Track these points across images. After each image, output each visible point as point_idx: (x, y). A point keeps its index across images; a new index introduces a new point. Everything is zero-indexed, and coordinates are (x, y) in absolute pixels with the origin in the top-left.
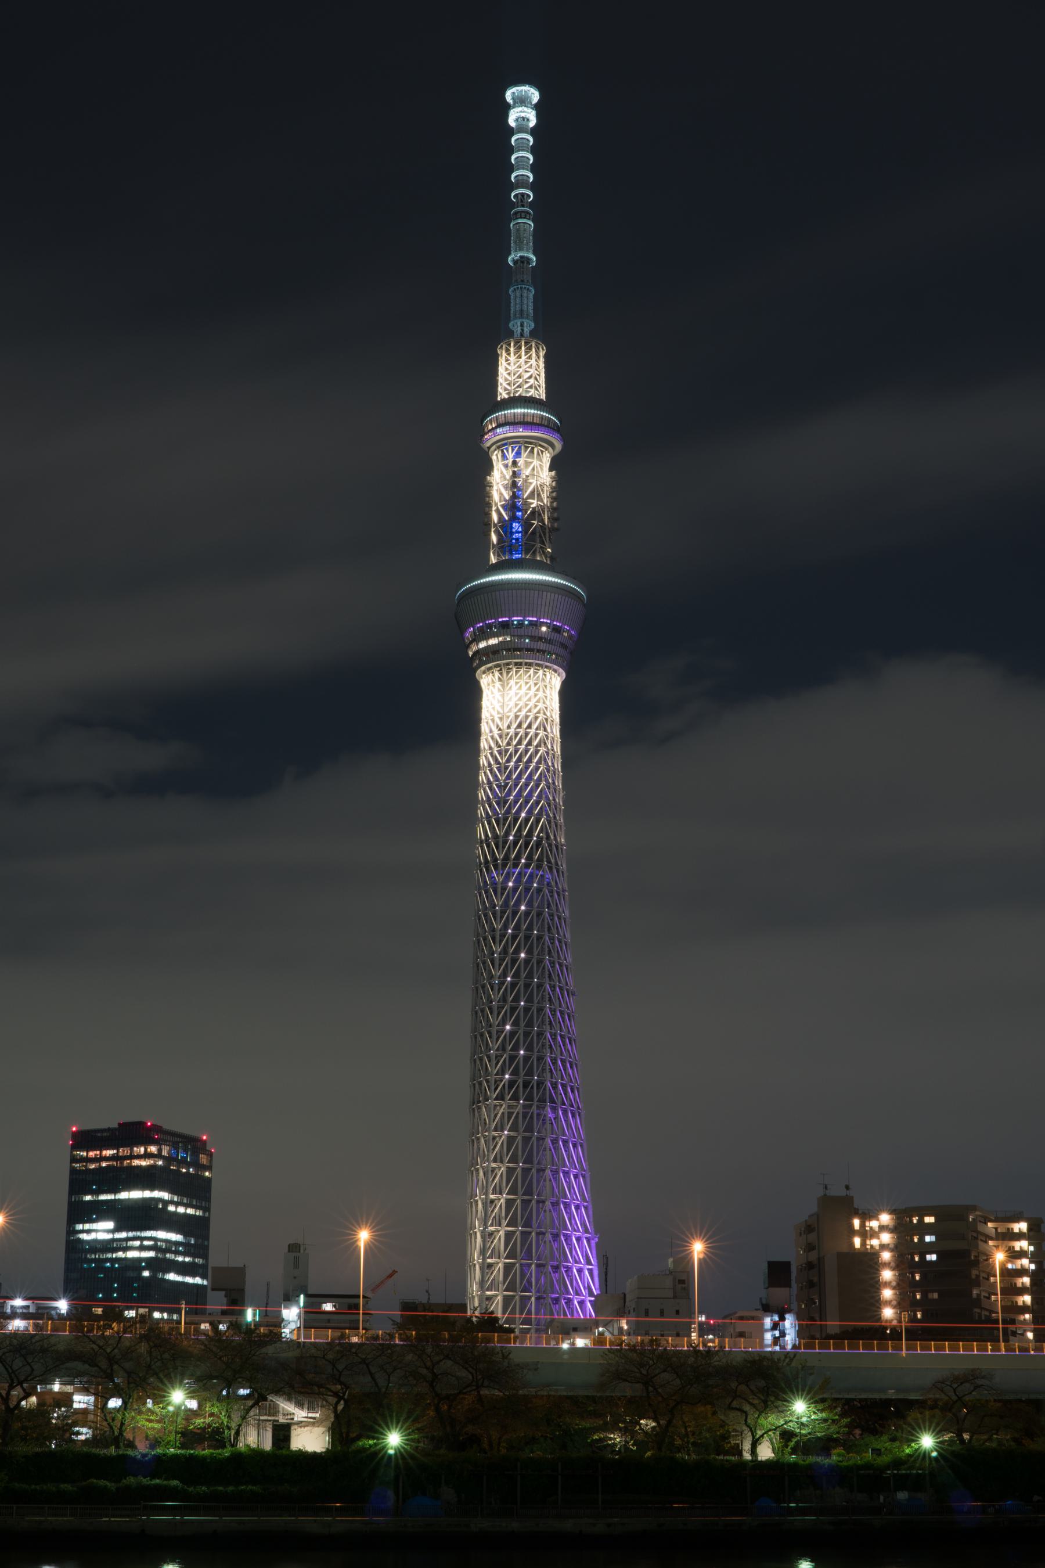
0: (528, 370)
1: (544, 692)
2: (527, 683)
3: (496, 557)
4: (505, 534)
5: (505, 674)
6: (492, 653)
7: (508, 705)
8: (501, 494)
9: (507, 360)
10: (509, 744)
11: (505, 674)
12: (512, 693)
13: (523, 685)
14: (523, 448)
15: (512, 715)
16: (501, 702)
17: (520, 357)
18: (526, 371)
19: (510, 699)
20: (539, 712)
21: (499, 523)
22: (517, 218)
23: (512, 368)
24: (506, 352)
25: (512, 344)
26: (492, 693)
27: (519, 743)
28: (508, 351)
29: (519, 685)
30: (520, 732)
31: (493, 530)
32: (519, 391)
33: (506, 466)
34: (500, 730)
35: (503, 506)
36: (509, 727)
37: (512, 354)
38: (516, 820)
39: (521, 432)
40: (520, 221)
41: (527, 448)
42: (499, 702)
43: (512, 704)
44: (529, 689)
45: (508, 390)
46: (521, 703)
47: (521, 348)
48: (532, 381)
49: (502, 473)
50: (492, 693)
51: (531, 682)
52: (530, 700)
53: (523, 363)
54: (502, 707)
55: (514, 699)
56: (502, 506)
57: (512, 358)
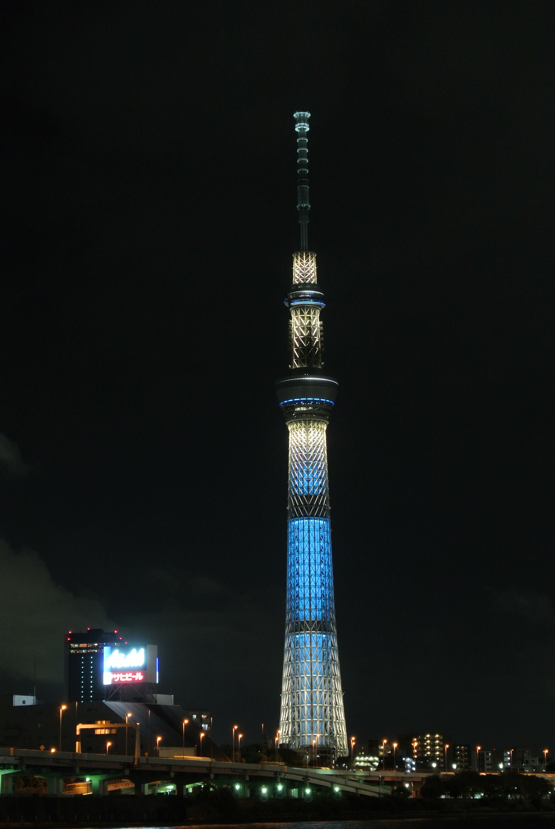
0: (312, 268)
1: (323, 434)
2: (318, 430)
3: (299, 364)
4: (305, 354)
5: (307, 425)
6: (301, 413)
7: (309, 441)
8: (301, 331)
9: (301, 261)
10: (311, 460)
11: (307, 425)
12: (311, 434)
13: (316, 431)
14: (312, 310)
15: (312, 445)
16: (306, 438)
17: (308, 261)
18: (312, 269)
19: (311, 438)
20: (322, 445)
21: (299, 346)
22: (302, 184)
24: (300, 257)
25: (304, 254)
26: (300, 433)
27: (315, 460)
28: (302, 257)
29: (314, 431)
30: (315, 454)
31: (294, 349)
32: (309, 279)
33: (303, 318)
34: (305, 452)
35: (303, 339)
36: (310, 452)
37: (304, 259)
38: (315, 497)
39: (311, 302)
40: (303, 186)
41: (313, 310)
42: (304, 438)
43: (311, 440)
44: (318, 433)
45: (302, 277)
46: (316, 440)
47: (309, 256)
48: (314, 274)
49: (300, 320)
50: (300, 433)
51: (319, 430)
52: (319, 439)
53: (310, 265)
54: (307, 440)
55: (313, 438)
56: (302, 339)
57: (304, 261)
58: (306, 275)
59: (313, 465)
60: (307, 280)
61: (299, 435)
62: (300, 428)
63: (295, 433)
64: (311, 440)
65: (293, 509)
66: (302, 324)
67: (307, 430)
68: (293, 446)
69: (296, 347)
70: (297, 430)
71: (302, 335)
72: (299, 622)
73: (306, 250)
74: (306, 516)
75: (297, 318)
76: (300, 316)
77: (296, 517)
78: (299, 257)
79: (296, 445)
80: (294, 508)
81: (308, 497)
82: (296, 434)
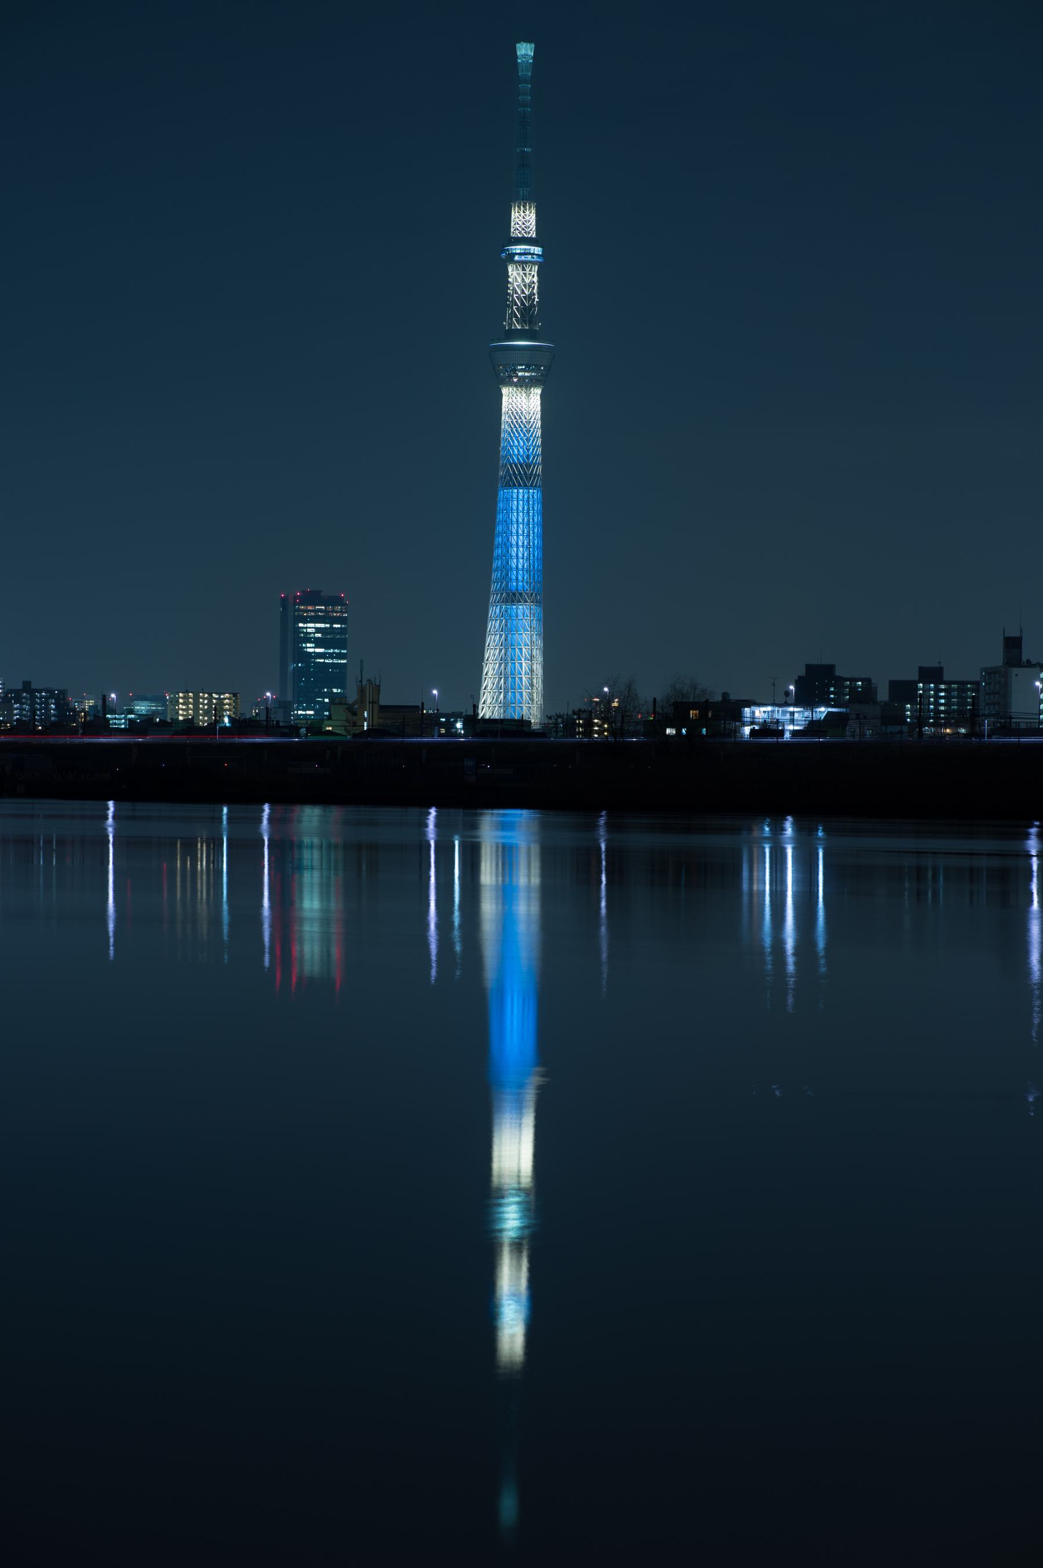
8: (522, 289)
10: (530, 428)
12: (531, 401)
15: (532, 412)
23: (527, 218)
27: (535, 428)
33: (525, 274)
36: (530, 419)
42: (525, 404)
49: (522, 277)
50: (521, 398)
55: (533, 404)
58: (529, 227)
59: (533, 433)
60: (529, 233)
61: (519, 400)
62: (521, 393)
63: (514, 398)
64: (531, 407)
65: (511, 478)
66: (523, 279)
67: (528, 396)
68: (511, 410)
69: (516, 304)
70: (517, 395)
71: (523, 292)
72: (517, 594)
73: (523, 199)
74: (525, 485)
75: (519, 274)
76: (521, 273)
77: (514, 485)
78: (522, 207)
79: (516, 410)
80: (512, 477)
81: (528, 466)
82: (516, 398)
